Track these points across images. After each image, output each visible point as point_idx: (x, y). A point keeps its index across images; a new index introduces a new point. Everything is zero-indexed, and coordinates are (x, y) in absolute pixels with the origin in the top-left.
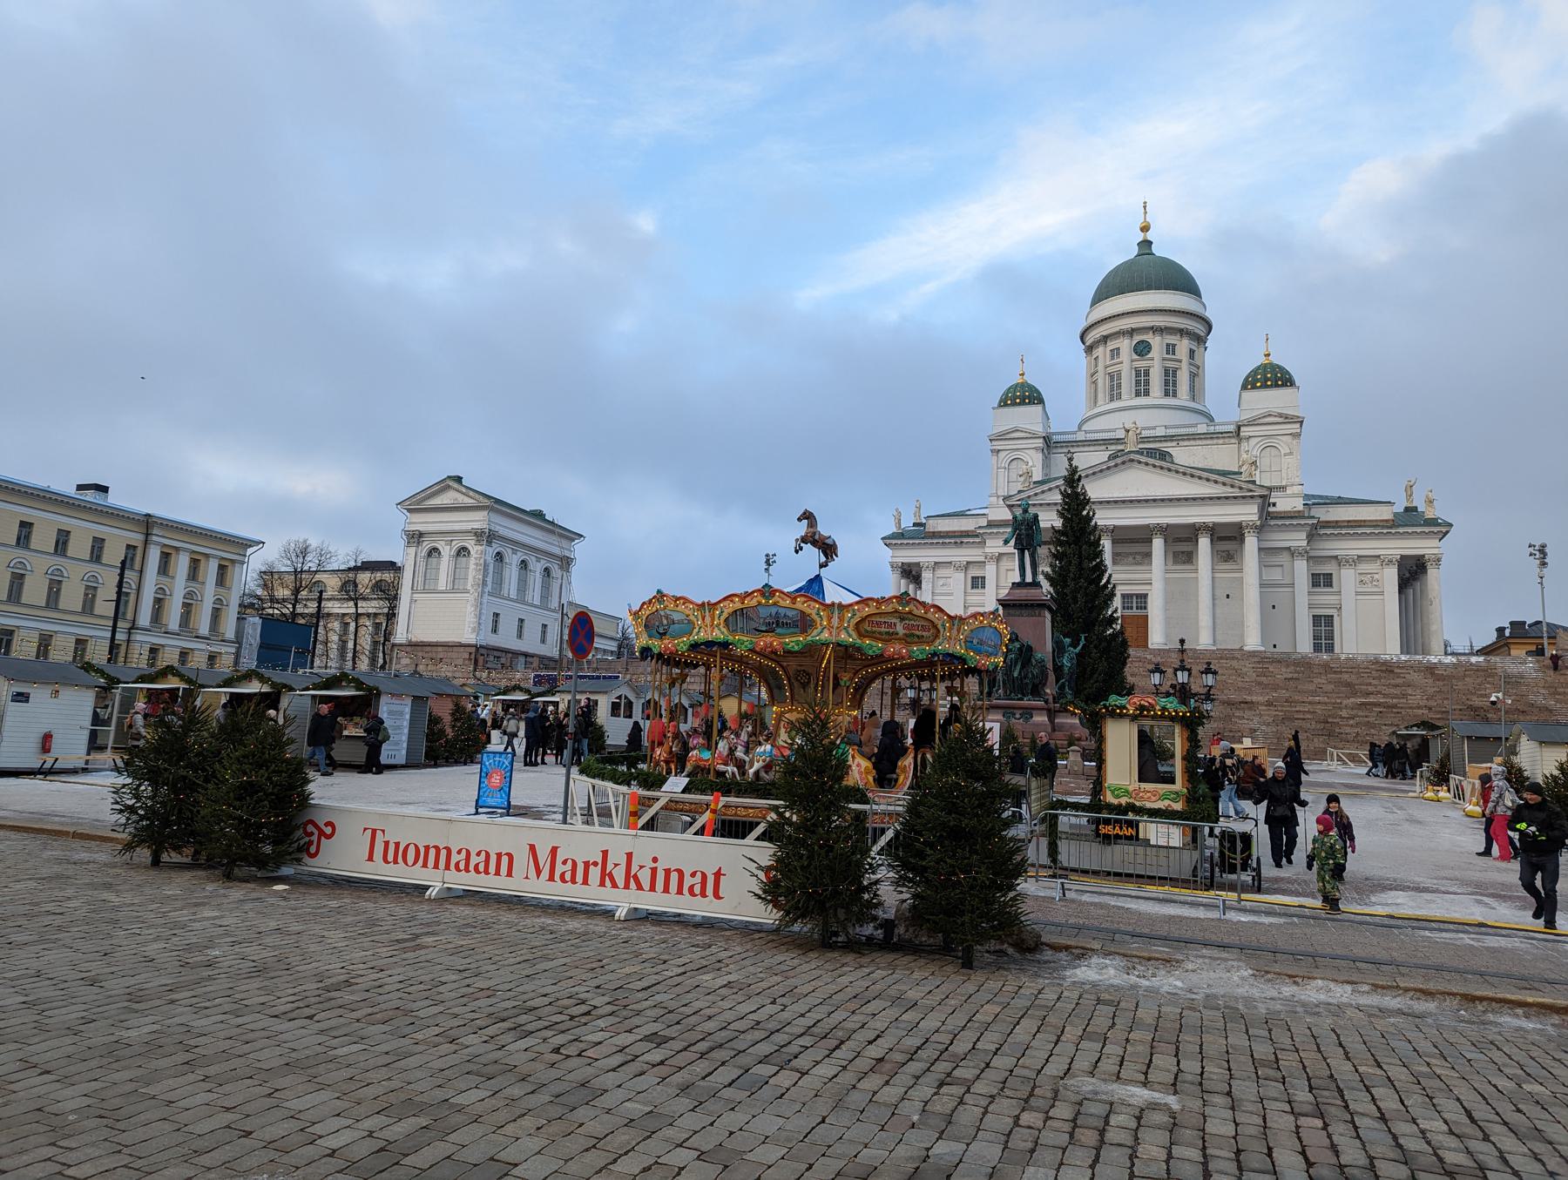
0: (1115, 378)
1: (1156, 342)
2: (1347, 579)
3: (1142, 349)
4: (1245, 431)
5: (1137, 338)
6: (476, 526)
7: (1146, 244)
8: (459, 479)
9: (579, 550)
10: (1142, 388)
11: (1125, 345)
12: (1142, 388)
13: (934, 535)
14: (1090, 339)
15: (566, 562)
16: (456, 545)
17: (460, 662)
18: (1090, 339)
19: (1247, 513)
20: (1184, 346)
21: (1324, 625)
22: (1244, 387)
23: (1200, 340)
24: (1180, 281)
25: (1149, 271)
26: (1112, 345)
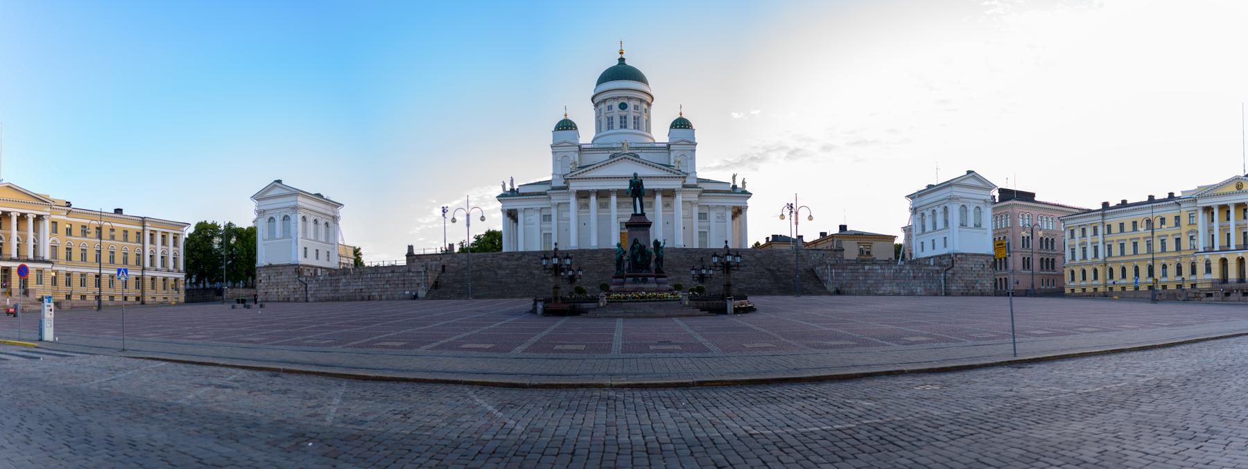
1: (631, 104)
2: (713, 215)
3: (623, 106)
4: (672, 147)
7: (622, 60)
10: (624, 124)
11: (616, 104)
12: (624, 124)
13: (523, 194)
14: (596, 100)
18: (596, 100)
19: (676, 184)
21: (703, 234)
22: (671, 127)
25: (622, 72)
26: (608, 103)
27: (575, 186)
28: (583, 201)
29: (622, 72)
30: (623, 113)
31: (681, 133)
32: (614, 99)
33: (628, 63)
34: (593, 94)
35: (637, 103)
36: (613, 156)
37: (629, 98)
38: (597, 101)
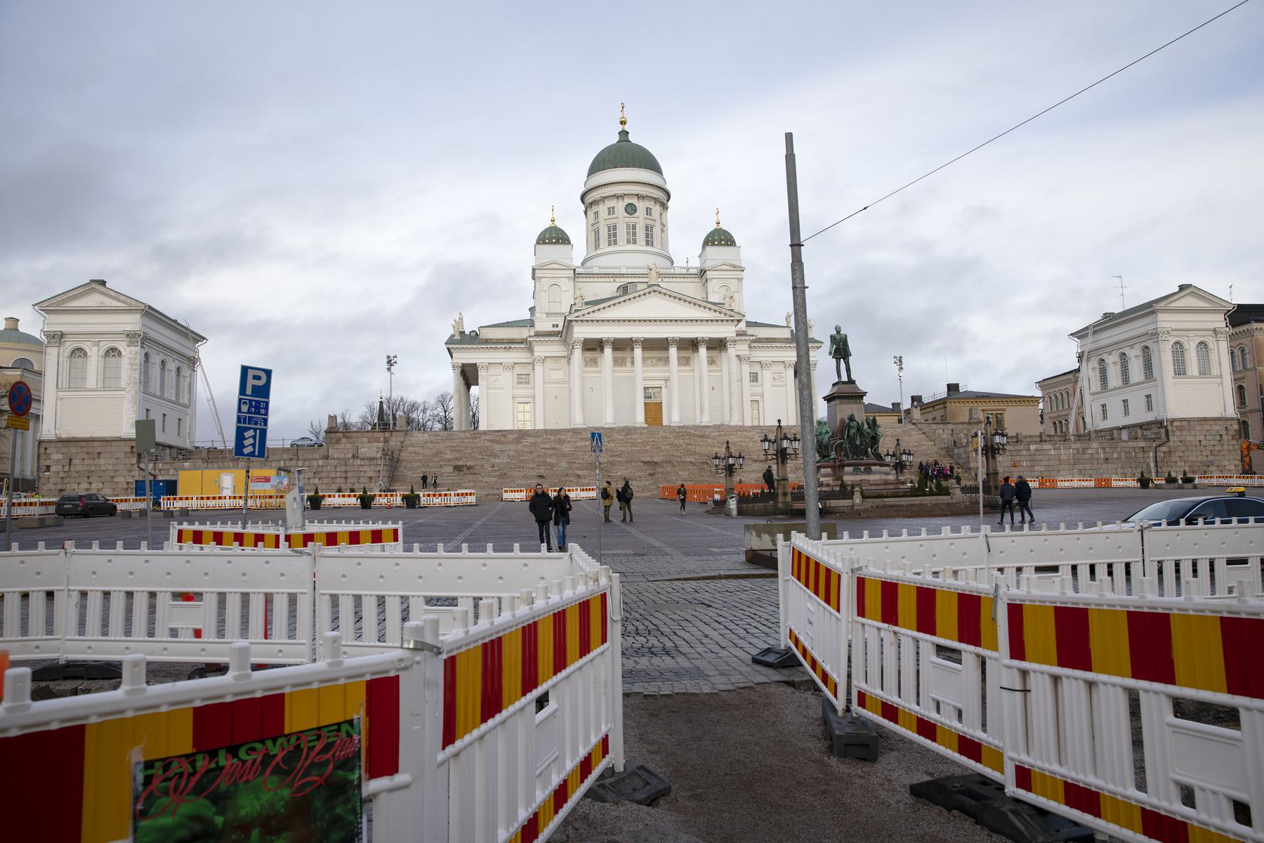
0: (612, 231)
1: (641, 206)
2: (766, 376)
3: (631, 209)
4: (709, 274)
5: (627, 201)
6: (129, 328)
7: (624, 134)
8: (103, 283)
9: (203, 351)
13: (487, 341)
14: (589, 199)
15: (193, 362)
16: (105, 346)
17: (121, 455)
19: (727, 331)
20: (657, 209)
23: (664, 206)
24: (647, 161)
25: (625, 154)
26: (609, 204)
27: (581, 332)
28: (589, 355)
29: (625, 154)
30: (632, 220)
31: (718, 254)
32: (617, 197)
33: (633, 138)
34: (582, 189)
35: (650, 204)
36: (624, 289)
37: (638, 196)
38: (588, 200)
